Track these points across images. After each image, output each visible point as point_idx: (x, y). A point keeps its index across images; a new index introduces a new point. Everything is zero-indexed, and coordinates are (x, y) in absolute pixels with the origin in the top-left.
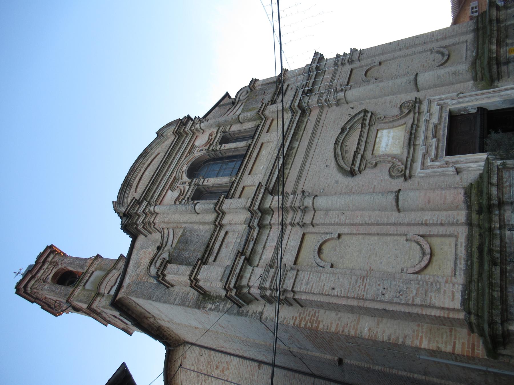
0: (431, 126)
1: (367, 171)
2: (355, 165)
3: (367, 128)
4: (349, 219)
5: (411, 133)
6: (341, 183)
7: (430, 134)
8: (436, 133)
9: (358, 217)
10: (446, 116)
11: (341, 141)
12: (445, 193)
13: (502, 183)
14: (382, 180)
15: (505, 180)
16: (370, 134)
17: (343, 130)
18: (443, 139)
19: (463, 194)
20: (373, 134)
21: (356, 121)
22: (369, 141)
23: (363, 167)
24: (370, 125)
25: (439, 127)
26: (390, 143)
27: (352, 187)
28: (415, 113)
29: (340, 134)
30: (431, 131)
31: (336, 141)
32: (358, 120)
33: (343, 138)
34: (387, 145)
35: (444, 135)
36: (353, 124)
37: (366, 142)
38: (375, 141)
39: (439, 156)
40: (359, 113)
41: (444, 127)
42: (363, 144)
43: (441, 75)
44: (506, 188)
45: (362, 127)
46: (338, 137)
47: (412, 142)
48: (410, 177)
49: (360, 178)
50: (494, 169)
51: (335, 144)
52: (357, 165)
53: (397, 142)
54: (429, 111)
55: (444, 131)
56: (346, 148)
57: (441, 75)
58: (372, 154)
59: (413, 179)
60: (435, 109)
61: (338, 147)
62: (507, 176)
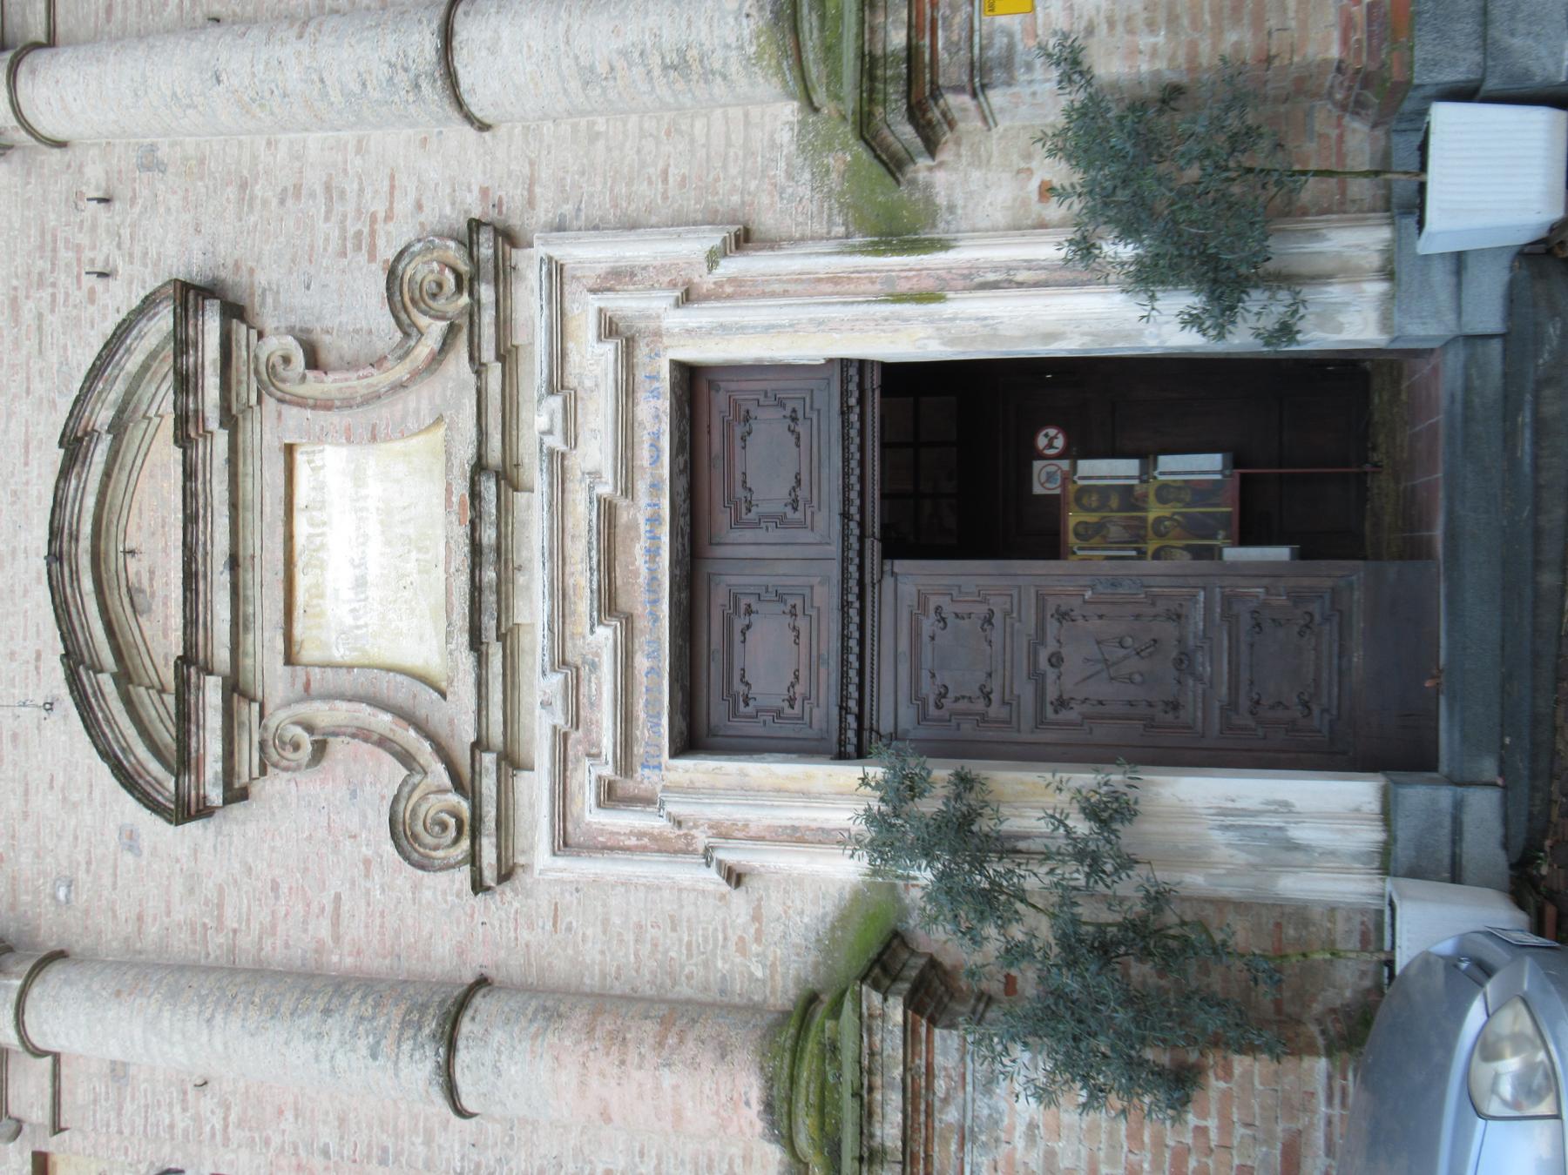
0: (581, 513)
1: (273, 787)
2: (200, 761)
3: (221, 439)
4: (239, 1126)
5: (476, 549)
6: (154, 851)
7: (583, 605)
8: (610, 569)
9: (281, 1112)
10: (655, 412)
11: (86, 529)
12: (676, 1087)
13: (929, 1114)
14: (367, 862)
15: (940, 1085)
16: (248, 487)
17: (74, 445)
18: (656, 619)
19: (756, 1107)
20: (264, 479)
21: (145, 367)
22: (251, 543)
23: (247, 759)
24: (230, 420)
25: (623, 517)
26: (373, 572)
27: (221, 890)
28: (479, 369)
29: (64, 474)
30: (584, 566)
31: (55, 533)
32: (153, 355)
33: (90, 502)
34: (361, 584)
35: (653, 579)
36: (129, 394)
37: (234, 563)
38: (289, 538)
39: (639, 750)
40: (148, 305)
41: (654, 520)
42: (221, 578)
43: (602, 69)
44: (945, 1141)
45: (183, 439)
46: (58, 504)
47: (489, 623)
48: (506, 874)
49: (251, 829)
50: (888, 1051)
51: (55, 557)
52: (213, 767)
53: (411, 566)
54: (557, 385)
55: (653, 553)
56: (133, 565)
57: (602, 69)
58: (289, 659)
59: (521, 878)
60: (593, 360)
61: (75, 575)
62: (950, 1064)
